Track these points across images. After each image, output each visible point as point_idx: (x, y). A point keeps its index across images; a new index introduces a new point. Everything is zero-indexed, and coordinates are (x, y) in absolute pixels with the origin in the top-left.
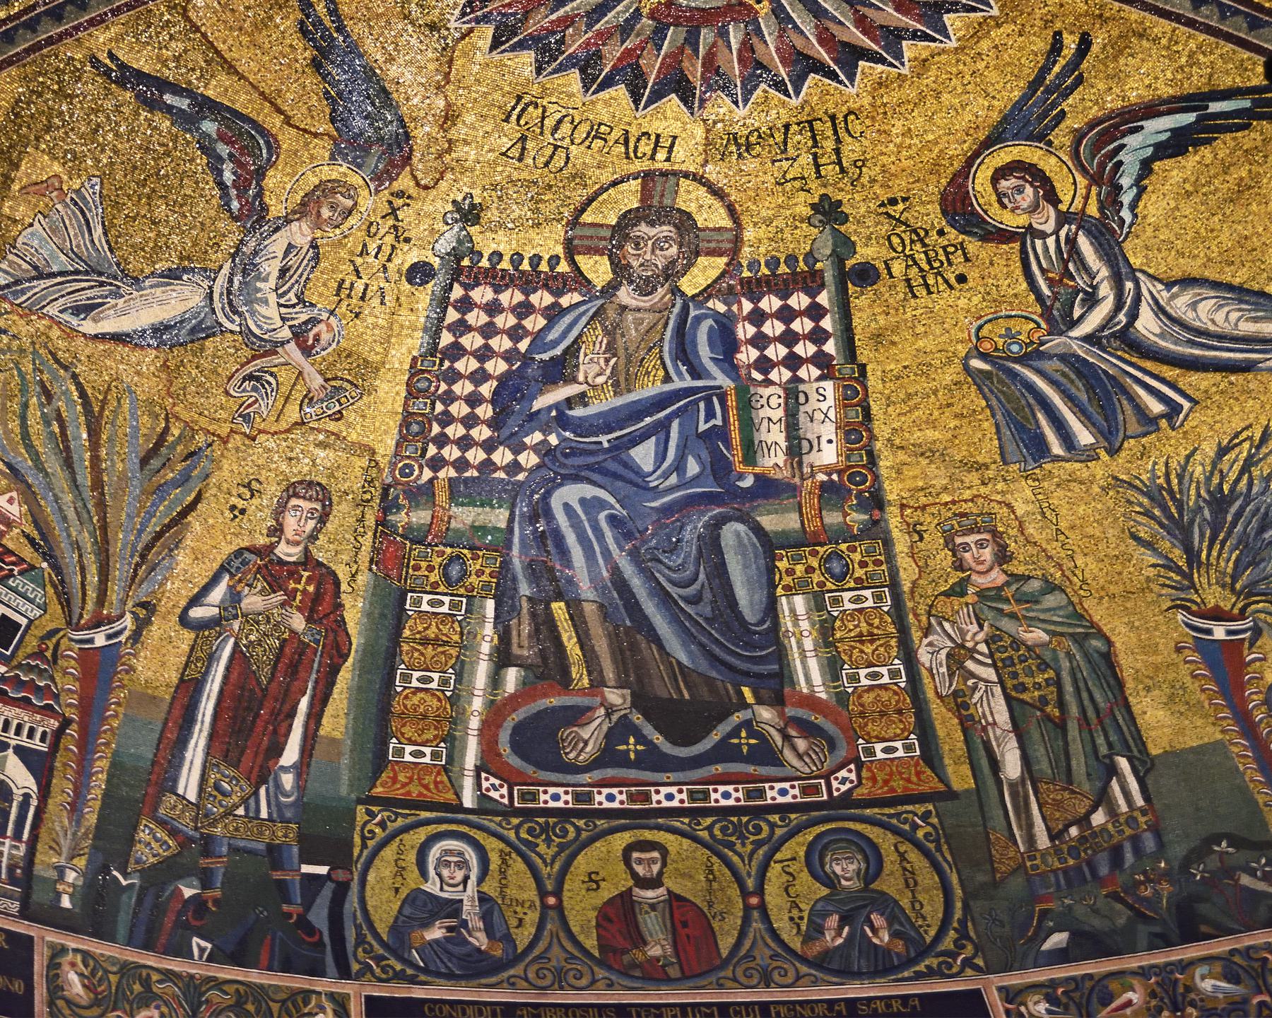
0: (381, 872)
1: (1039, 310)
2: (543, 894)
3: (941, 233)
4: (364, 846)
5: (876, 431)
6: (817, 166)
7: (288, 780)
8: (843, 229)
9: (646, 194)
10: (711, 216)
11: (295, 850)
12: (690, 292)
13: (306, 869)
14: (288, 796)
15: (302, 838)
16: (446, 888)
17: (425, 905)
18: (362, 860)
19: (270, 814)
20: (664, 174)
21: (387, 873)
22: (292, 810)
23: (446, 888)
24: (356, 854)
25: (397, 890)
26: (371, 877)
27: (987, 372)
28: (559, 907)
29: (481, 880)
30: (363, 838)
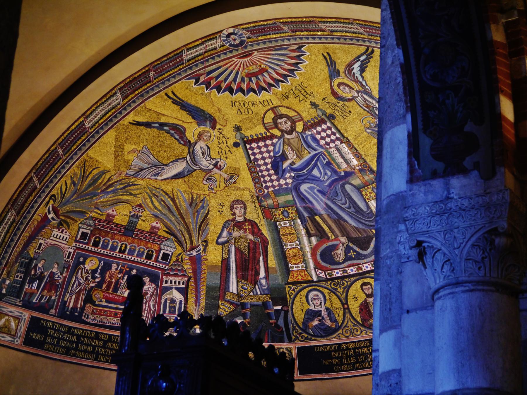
0: (297, 306)
1: (369, 114)
2: (343, 304)
3: (338, 103)
4: (290, 298)
5: (361, 153)
6: (305, 96)
7: (263, 282)
8: (320, 107)
9: (274, 113)
10: (292, 114)
11: (271, 303)
12: (301, 131)
13: (275, 308)
14: (265, 287)
15: (272, 299)
16: (316, 307)
17: (311, 314)
18: (291, 302)
19: (261, 293)
20: (275, 107)
21: (298, 305)
22: (267, 290)
23: (316, 307)
24: (288, 301)
25: (302, 310)
26: (294, 307)
27: (371, 132)
28: (348, 308)
29: (325, 303)
30: (290, 295)
